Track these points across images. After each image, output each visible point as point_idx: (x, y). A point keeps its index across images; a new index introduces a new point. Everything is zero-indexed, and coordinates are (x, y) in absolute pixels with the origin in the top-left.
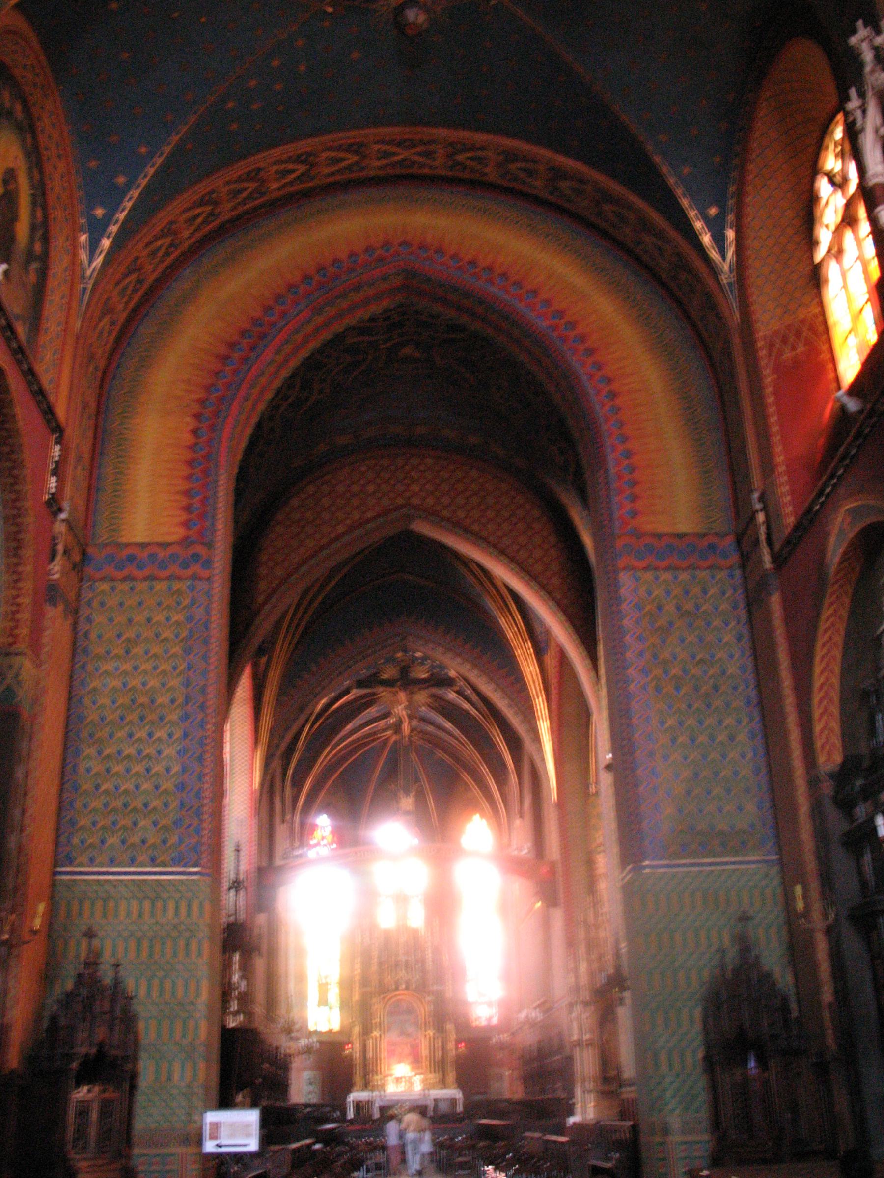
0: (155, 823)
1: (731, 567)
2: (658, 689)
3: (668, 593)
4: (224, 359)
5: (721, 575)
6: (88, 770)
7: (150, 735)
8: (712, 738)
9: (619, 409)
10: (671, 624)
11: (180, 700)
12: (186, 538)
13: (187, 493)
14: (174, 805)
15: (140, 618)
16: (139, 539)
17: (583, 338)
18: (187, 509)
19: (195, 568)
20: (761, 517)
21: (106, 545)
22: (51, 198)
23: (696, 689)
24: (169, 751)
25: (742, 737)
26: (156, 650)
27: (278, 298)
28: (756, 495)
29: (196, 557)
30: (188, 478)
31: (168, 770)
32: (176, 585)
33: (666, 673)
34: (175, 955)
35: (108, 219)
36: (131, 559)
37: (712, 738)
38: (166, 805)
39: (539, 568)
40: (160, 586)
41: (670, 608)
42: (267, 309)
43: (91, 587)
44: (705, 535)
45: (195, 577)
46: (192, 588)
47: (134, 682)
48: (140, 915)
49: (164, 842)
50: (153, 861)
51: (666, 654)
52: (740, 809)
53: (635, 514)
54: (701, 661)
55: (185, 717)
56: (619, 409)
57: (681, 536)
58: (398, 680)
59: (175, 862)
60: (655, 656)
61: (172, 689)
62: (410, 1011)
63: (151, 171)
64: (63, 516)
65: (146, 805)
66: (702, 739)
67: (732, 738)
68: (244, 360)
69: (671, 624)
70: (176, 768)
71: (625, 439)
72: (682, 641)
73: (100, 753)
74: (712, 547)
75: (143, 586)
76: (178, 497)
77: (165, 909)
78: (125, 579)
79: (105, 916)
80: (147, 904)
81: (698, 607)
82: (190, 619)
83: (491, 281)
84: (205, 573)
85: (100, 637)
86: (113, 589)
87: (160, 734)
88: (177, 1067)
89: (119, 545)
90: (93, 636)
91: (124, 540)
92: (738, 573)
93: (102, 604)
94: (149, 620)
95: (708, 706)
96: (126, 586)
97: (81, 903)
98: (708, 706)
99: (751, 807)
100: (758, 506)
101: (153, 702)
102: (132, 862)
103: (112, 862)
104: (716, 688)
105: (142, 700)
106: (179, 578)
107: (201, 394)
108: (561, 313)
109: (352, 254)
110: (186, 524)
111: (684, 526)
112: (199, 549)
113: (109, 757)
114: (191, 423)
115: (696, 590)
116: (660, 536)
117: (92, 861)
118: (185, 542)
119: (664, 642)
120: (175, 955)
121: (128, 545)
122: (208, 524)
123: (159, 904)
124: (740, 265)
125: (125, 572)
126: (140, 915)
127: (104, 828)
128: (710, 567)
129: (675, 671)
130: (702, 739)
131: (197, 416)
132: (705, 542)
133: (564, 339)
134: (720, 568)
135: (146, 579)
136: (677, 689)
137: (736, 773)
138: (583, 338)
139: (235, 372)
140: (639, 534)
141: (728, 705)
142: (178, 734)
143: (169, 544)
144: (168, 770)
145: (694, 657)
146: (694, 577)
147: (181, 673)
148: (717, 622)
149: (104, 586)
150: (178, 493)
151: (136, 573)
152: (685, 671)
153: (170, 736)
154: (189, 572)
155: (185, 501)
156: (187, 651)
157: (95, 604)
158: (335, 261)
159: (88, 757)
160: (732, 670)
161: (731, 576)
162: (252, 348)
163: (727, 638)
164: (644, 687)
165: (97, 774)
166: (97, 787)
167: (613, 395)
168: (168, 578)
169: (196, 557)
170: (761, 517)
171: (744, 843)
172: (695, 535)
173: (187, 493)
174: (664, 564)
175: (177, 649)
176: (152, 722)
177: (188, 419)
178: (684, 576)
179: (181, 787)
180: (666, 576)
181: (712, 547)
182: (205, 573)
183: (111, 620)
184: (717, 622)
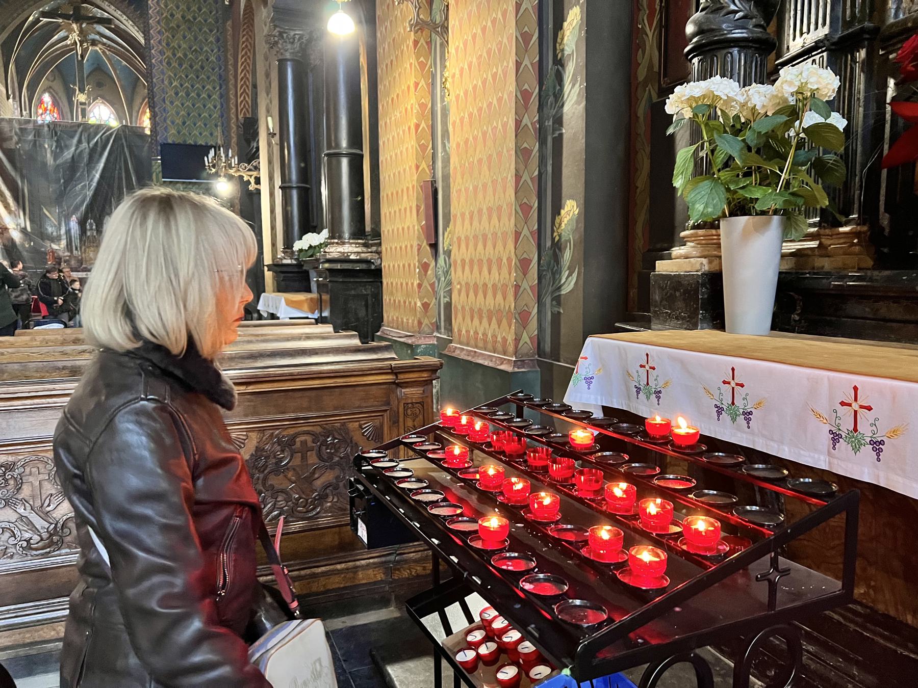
2: (169, 63)
8: (199, 95)
10: (178, 27)
23: (191, 67)
33: (174, 55)
37: (199, 95)
41: (178, 16)
58: (71, 16)
60: (168, 44)
67: (209, 96)
69: (178, 27)
72: (185, 37)
81: (195, 19)
95: (198, 77)
98: (198, 77)
129: (180, 55)
136: (180, 65)
141: (208, 78)
145: (191, 48)
152: (185, 55)
163: (211, 39)
164: (161, 62)
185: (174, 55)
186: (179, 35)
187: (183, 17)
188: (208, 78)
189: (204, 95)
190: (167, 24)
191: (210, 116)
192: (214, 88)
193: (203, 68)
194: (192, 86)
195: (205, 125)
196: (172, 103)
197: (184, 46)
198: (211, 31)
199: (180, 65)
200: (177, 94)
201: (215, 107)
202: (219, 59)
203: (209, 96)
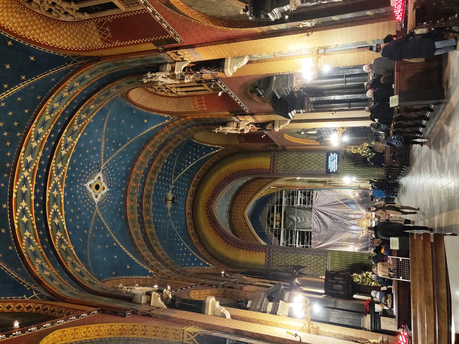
0: (320, 260)
3: (282, 165)
4: (228, 243)
5: (279, 155)
6: (309, 272)
7: (303, 260)
8: (309, 160)
10: (288, 165)
11: (296, 254)
12: (265, 252)
13: (256, 251)
23: (300, 162)
24: (306, 257)
26: (287, 258)
29: (269, 250)
30: (253, 251)
31: (310, 257)
32: (274, 254)
33: (297, 167)
34: (344, 257)
36: (268, 262)
37: (309, 160)
38: (316, 258)
40: (274, 257)
41: (284, 165)
42: (219, 234)
46: (275, 251)
49: (323, 258)
57: (271, 162)
60: (293, 169)
61: (294, 256)
65: (316, 261)
66: (309, 162)
70: (309, 255)
74: (273, 156)
77: (335, 259)
80: (334, 262)
81: (285, 160)
82: (281, 252)
87: (303, 258)
94: (281, 260)
96: (274, 264)
99: (322, 155)
101: (297, 259)
102: (327, 264)
106: (273, 253)
107: (235, 248)
108: (224, 179)
109: (208, 217)
110: (262, 252)
111: (269, 161)
114: (242, 250)
115: (282, 160)
116: (270, 165)
118: (266, 252)
120: (344, 257)
123: (335, 260)
126: (337, 263)
127: (320, 269)
128: (277, 157)
129: (296, 165)
130: (309, 162)
132: (272, 157)
134: (278, 155)
136: (300, 165)
137: (316, 157)
140: (270, 169)
141: (303, 157)
144: (310, 257)
148: (288, 157)
152: (297, 163)
153: (303, 256)
154: (272, 251)
155: (257, 252)
156: (287, 253)
159: (306, 272)
160: (297, 155)
161: (279, 153)
163: (291, 155)
166: (312, 270)
173: (256, 251)
174: (276, 165)
177: (241, 250)
178: (279, 162)
179: (313, 255)
185: (297, 167)
187: (285, 163)
188: (303, 157)
189: (309, 158)
190: (287, 168)
191: (316, 157)
192: (307, 155)
193: (300, 158)
194: (306, 162)
195: (319, 158)
196: (312, 169)
197: (293, 164)
198: (288, 155)
199: (300, 165)
201: (313, 155)
202: (297, 153)
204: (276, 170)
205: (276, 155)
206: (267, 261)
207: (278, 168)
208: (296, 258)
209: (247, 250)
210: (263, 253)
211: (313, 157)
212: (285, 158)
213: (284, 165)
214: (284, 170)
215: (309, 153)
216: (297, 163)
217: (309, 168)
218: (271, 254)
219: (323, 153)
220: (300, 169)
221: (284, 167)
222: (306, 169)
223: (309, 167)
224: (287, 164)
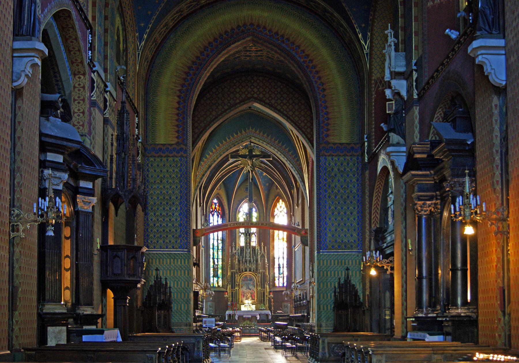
0: (173, 236)
1: (358, 155)
5: (354, 158)
6: (151, 220)
7: (170, 209)
8: (345, 213)
9: (326, 96)
11: (179, 197)
13: (177, 126)
14: (179, 230)
15: (165, 170)
16: (163, 143)
17: (315, 67)
18: (177, 132)
19: (181, 153)
20: (366, 144)
21: (151, 145)
22: (127, 24)
25: (355, 213)
26: (170, 181)
27: (206, 48)
28: (365, 136)
29: (181, 149)
31: (176, 220)
34: (181, 275)
35: (146, 27)
36: (160, 149)
37: (345, 213)
38: (176, 231)
39: (303, 125)
40: (171, 159)
41: (336, 169)
43: (148, 160)
44: (350, 144)
45: (182, 156)
46: (181, 160)
47: (164, 192)
48: (170, 263)
49: (176, 242)
50: (173, 247)
51: (333, 185)
52: (352, 236)
53: (328, 136)
54: (345, 188)
55: (181, 203)
56: (326, 96)
59: (179, 248)
60: (329, 186)
62: (251, 279)
63: (160, 9)
64: (140, 141)
67: (351, 213)
68: (194, 74)
70: (179, 219)
71: (326, 107)
72: (339, 181)
73: (155, 214)
75: (165, 159)
76: (175, 127)
77: (177, 261)
78: (158, 157)
79: (159, 263)
80: (172, 260)
81: (345, 170)
82: (181, 170)
83: (283, 42)
84: (185, 155)
85: (152, 176)
86: (155, 160)
87: (174, 208)
88: (183, 305)
89: (155, 144)
90: (150, 176)
91: (157, 143)
92: (360, 157)
93: (152, 165)
95: (345, 203)
97: (152, 260)
98: (345, 203)
99: (355, 235)
100: (366, 140)
101: (170, 198)
103: (161, 248)
104: (348, 197)
105: (167, 197)
106: (176, 157)
108: (308, 56)
111: (344, 141)
112: (182, 146)
113: (158, 215)
115: (345, 164)
116: (335, 144)
117: (155, 248)
118: (178, 143)
119: (332, 181)
120: (181, 275)
121: (158, 145)
122: (185, 137)
123: (176, 260)
124: (371, 48)
125: (158, 155)
126: (170, 263)
128: (351, 156)
130: (342, 213)
131: (179, 97)
133: (308, 67)
134: (354, 156)
135: (165, 157)
136: (336, 197)
137: (351, 225)
138: (315, 67)
139: (191, 79)
140: (328, 143)
142: (179, 208)
143: (172, 145)
144: (176, 220)
145: (342, 186)
146: (345, 159)
147: (179, 189)
148: (351, 175)
149: (152, 159)
150: (173, 126)
151: (162, 154)
152: (339, 191)
153: (176, 209)
154: (180, 154)
156: (180, 182)
157: (149, 165)
158: (226, 32)
160: (354, 191)
161: (358, 159)
162: (197, 69)
163: (354, 180)
165: (155, 220)
167: (324, 90)
168: (173, 156)
169: (181, 149)
170: (366, 144)
171: (352, 246)
172: (347, 144)
173: (177, 126)
175: (177, 181)
176: (170, 205)
177: (176, 98)
178: (342, 158)
179: (180, 225)
180: (336, 158)
181: (352, 148)
182: (185, 155)
183: (155, 171)
184: (351, 175)
186: (336, 180)
187: (339, 170)
189: (348, 213)
193: (348, 197)
196: (330, 219)
197: (338, 185)
199: (336, 197)
200: (333, 214)
203: (351, 213)
204: (326, 154)
205: (355, 154)
206: (162, 147)
207: (330, 158)
208: (172, 197)
209: (178, 109)
210: (176, 140)
211: (351, 218)
212: (348, 169)
213: (336, 169)
214: (326, 169)
215: (358, 212)
216: (339, 191)
217: (330, 213)
218: (176, 154)
219: (358, 235)
220: (329, 197)
221: (332, 170)
222: (330, 208)
223: (333, 214)
224: (338, 175)
